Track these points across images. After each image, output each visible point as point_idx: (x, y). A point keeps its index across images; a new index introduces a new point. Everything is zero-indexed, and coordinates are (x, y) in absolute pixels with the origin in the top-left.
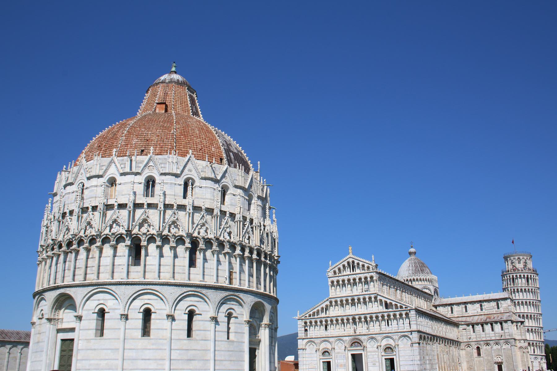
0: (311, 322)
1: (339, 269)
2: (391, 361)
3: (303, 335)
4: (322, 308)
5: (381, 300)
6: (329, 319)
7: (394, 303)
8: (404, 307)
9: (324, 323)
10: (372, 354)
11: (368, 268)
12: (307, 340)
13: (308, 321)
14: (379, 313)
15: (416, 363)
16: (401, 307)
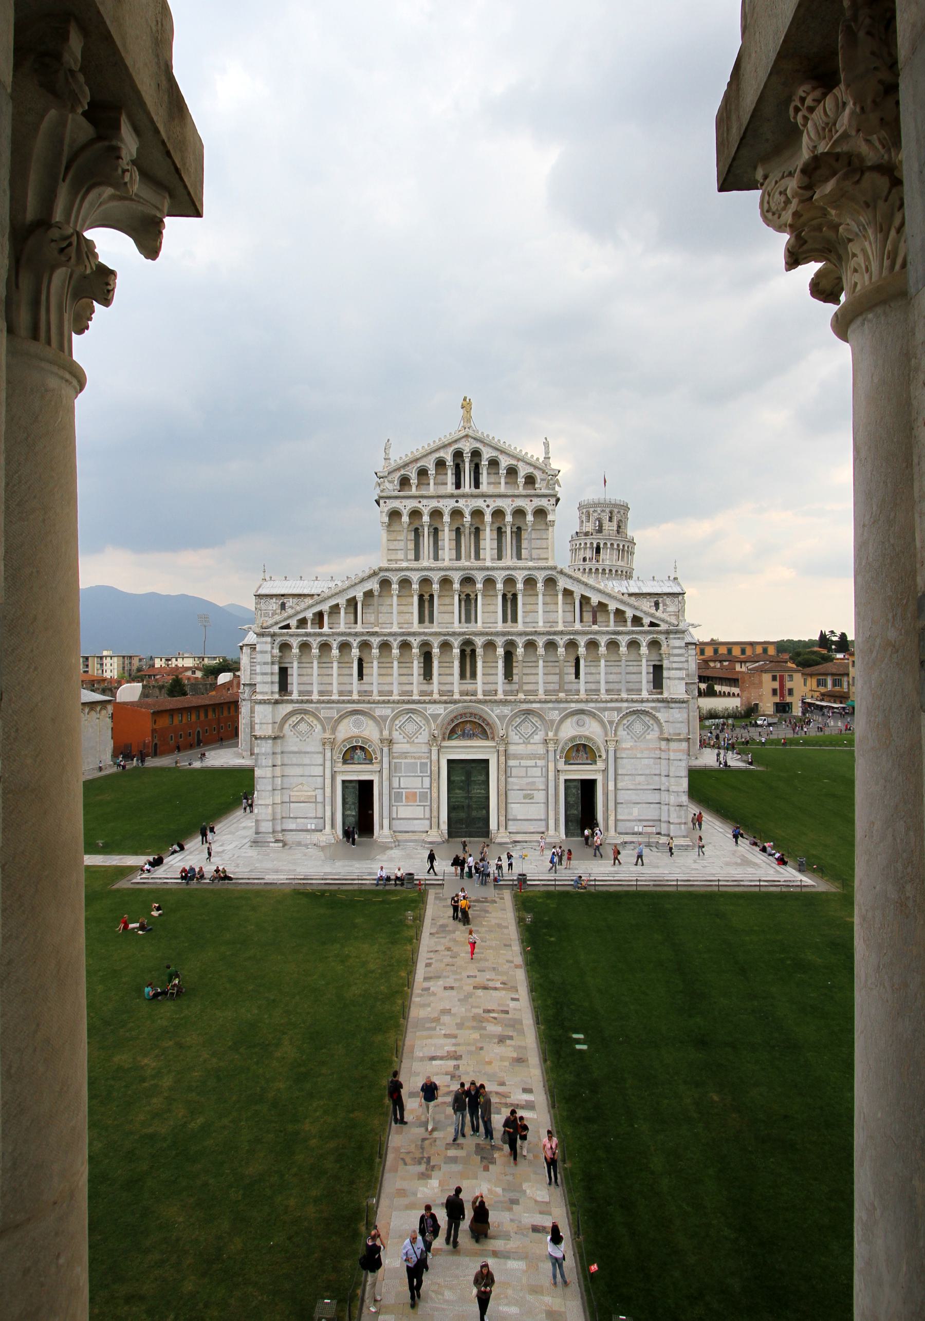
0: (305, 646)
1: (423, 472)
2: (588, 787)
3: (276, 688)
4: (352, 602)
5: (568, 593)
6: (375, 641)
7: (612, 606)
8: (646, 621)
9: (355, 652)
10: (524, 763)
11: (530, 480)
12: (289, 708)
13: (295, 643)
14: (562, 633)
15: (673, 799)
16: (637, 621)
